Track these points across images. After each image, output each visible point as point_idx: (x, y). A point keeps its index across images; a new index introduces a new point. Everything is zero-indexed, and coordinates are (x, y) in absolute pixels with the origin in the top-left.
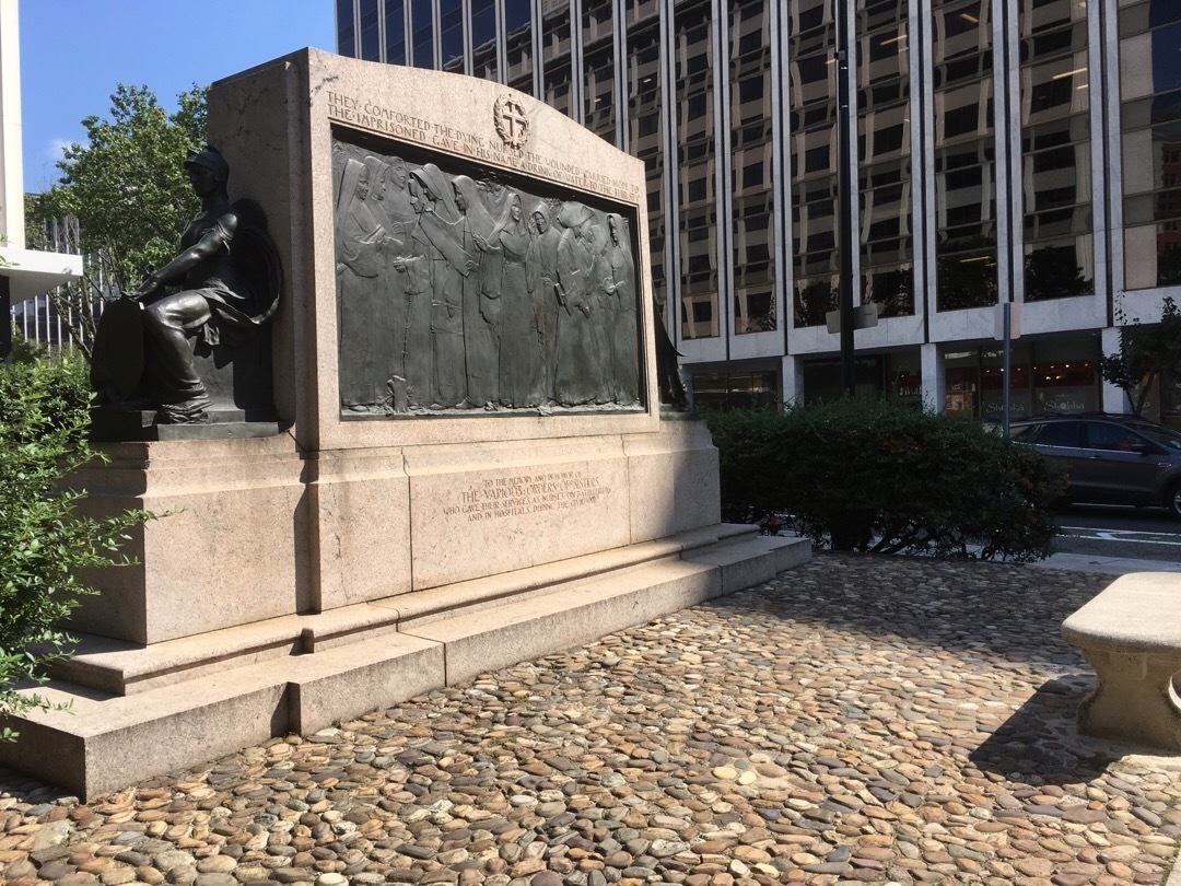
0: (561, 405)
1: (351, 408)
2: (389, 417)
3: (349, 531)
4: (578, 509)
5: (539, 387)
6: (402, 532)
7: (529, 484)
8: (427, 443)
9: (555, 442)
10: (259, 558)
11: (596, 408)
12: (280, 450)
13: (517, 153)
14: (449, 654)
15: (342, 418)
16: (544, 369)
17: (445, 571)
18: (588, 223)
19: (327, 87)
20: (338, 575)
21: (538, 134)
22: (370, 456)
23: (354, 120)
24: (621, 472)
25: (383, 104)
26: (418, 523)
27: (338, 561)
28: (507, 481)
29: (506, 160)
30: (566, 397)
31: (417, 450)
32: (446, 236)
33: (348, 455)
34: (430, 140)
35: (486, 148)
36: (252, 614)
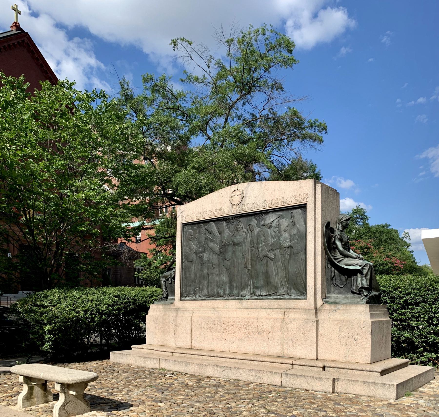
0: (256, 295)
1: (185, 297)
2: (192, 300)
3: (176, 329)
4: (252, 336)
5: (246, 289)
6: (189, 332)
7: (229, 323)
8: (201, 307)
9: (246, 310)
10: (163, 332)
11: (275, 297)
12: (171, 307)
13: (238, 206)
14: (161, 361)
15: (180, 300)
16: (249, 282)
17: (200, 345)
18: (277, 220)
19: (181, 215)
20: (174, 339)
21: (248, 195)
22: (184, 309)
23: (187, 221)
24: (278, 324)
25: (195, 212)
26: (193, 330)
27: (174, 336)
28: (221, 321)
29: (233, 211)
30: (258, 293)
31: (197, 309)
32: (213, 244)
33: (180, 309)
34: (207, 217)
35: (226, 210)
36: (162, 344)
